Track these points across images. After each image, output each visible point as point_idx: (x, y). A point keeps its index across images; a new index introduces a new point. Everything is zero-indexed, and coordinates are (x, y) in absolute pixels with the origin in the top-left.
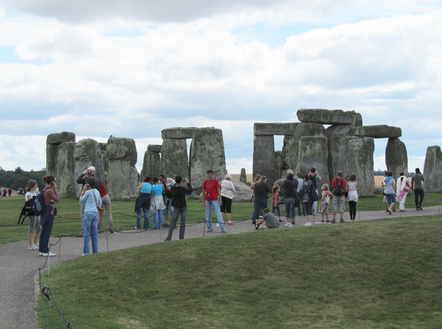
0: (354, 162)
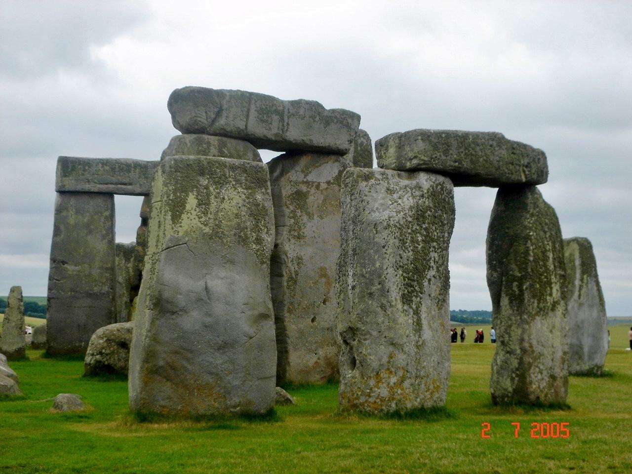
0: (379, 274)
